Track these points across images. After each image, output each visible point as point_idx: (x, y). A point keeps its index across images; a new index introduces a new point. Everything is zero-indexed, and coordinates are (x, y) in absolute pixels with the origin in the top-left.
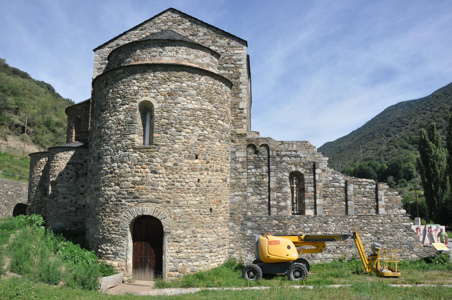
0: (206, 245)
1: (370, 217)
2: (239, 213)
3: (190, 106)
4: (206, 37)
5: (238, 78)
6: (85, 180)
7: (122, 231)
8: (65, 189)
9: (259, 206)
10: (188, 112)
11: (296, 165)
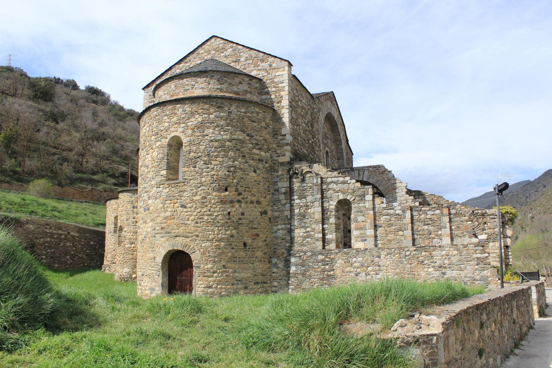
0: (239, 281)
1: (432, 248)
2: (283, 248)
3: (219, 137)
4: (248, 62)
5: (280, 102)
9: (305, 240)
10: (216, 144)
11: (343, 193)
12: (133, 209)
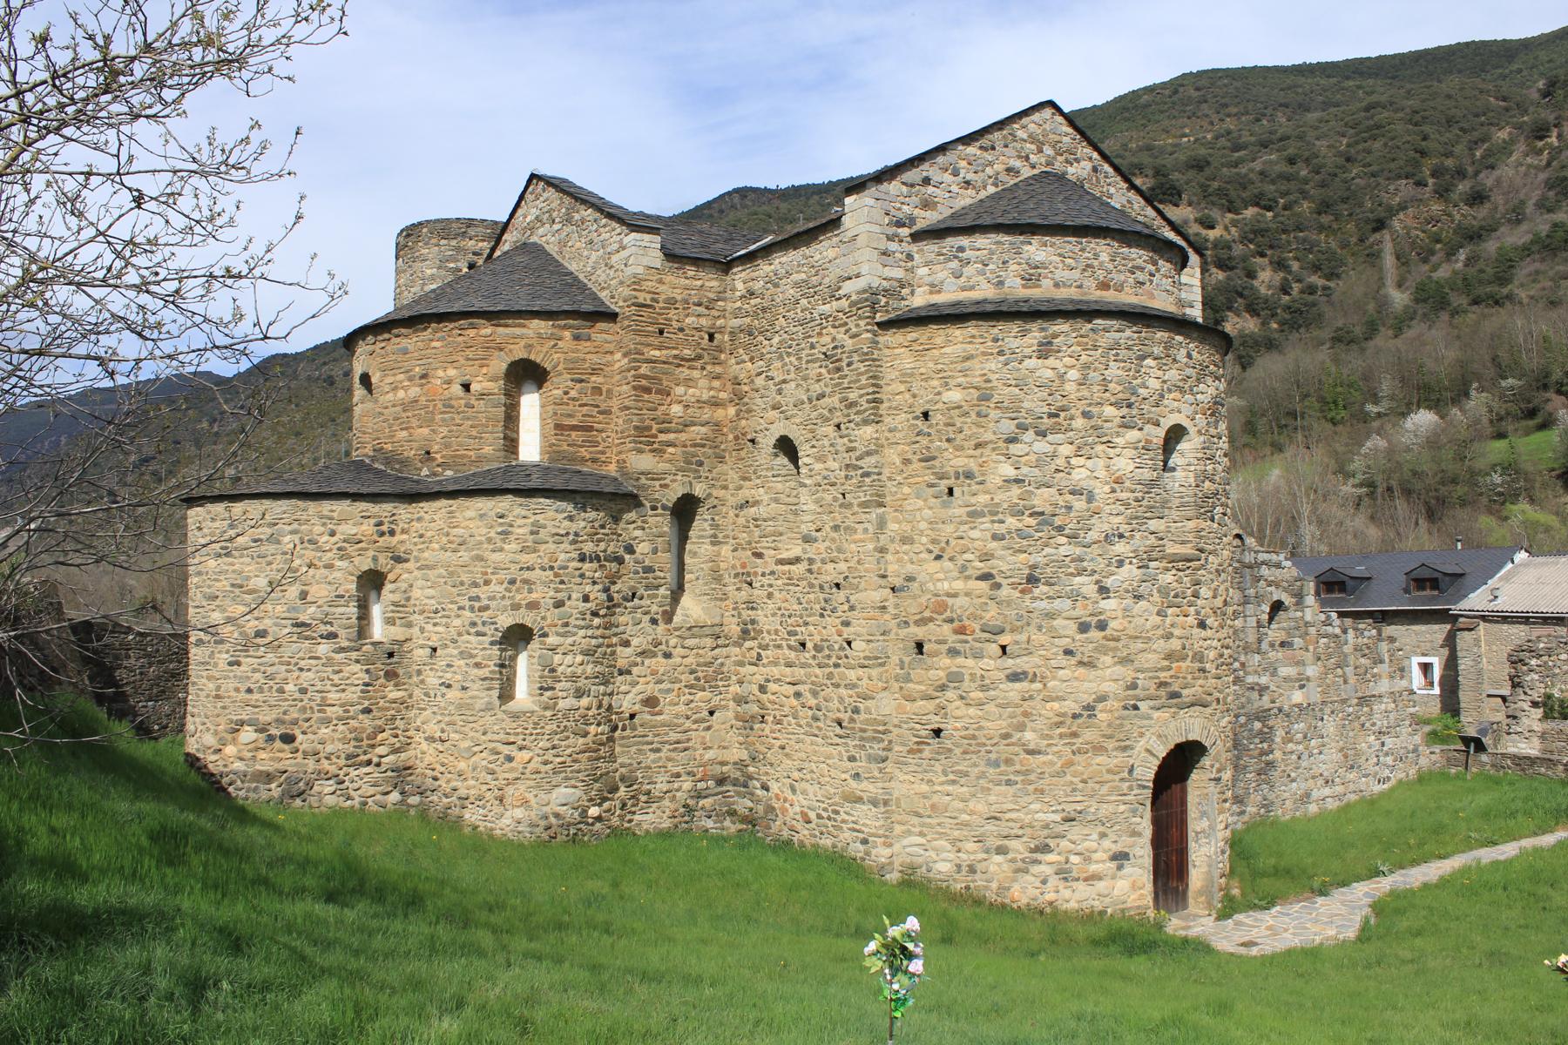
8: (579, 658)
12: (579, 565)
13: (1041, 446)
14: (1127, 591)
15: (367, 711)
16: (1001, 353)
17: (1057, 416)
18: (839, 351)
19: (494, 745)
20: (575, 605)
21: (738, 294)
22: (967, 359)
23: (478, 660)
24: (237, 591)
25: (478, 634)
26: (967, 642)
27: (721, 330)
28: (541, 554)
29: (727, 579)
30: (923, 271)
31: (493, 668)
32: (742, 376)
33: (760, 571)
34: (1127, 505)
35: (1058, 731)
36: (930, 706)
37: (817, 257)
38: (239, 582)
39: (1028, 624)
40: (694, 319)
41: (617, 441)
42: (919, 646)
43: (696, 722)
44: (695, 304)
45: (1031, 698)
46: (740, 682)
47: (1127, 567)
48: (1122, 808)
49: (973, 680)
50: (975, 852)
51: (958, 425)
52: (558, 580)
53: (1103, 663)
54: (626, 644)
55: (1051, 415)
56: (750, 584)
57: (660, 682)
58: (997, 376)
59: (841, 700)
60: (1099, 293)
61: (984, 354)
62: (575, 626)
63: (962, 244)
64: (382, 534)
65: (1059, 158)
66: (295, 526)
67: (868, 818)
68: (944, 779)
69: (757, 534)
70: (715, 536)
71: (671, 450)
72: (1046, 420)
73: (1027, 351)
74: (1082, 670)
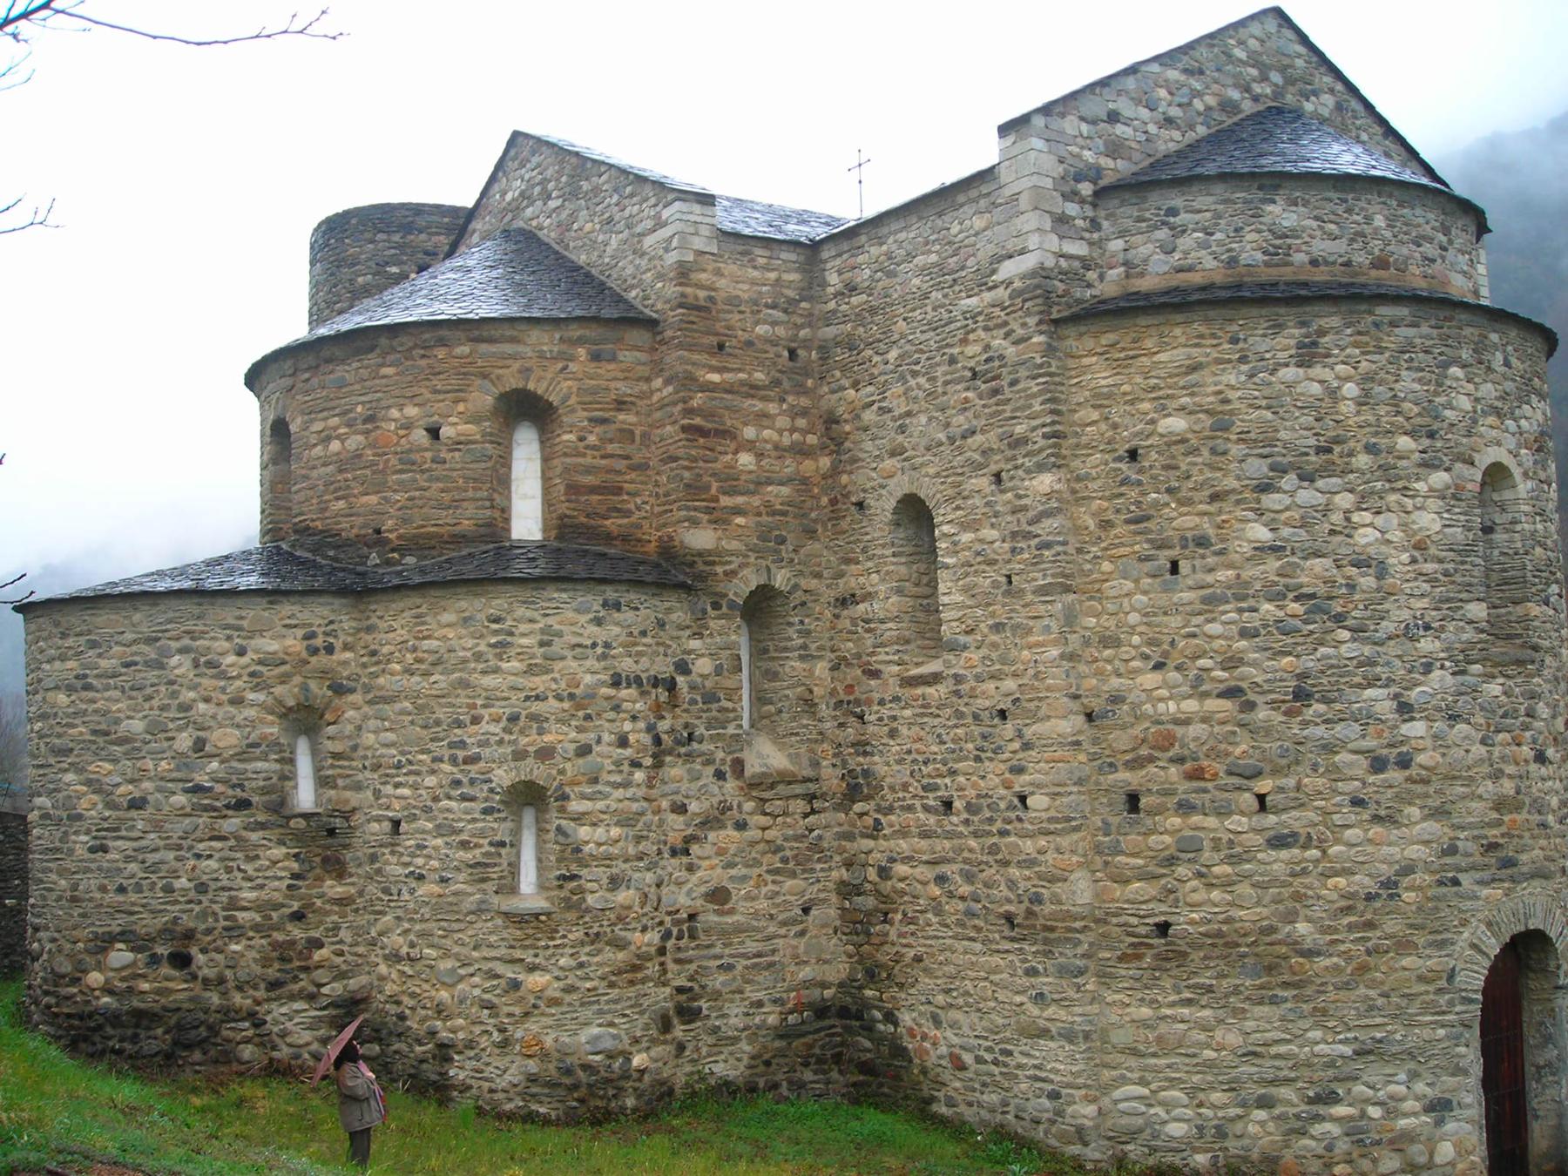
6: (689, 771)
7: (1462, 1008)
8: (615, 832)
12: (611, 692)
13: (1307, 496)
14: (1439, 709)
15: (298, 917)
16: (1243, 359)
17: (1329, 451)
18: (997, 363)
19: (490, 965)
20: (606, 754)
21: (831, 290)
22: (1194, 368)
23: (464, 837)
24: (100, 740)
25: (465, 798)
26: (1205, 791)
27: (807, 344)
28: (557, 676)
29: (824, 710)
30: (1117, 245)
31: (487, 848)
32: (841, 410)
33: (876, 696)
34: (1432, 581)
35: (1346, 921)
36: (1151, 889)
37: (955, 229)
38: (104, 727)
39: (1297, 762)
40: (767, 327)
41: (657, 509)
42: (1133, 801)
43: (784, 924)
44: (767, 306)
45: (1304, 872)
46: (848, 865)
47: (1437, 674)
48: (1441, 1032)
49: (1216, 849)
50: (1225, 1106)
51: (1184, 467)
52: (581, 714)
53: (1409, 816)
54: (680, 809)
55: (1320, 450)
56: (861, 717)
57: (730, 865)
58: (1239, 393)
59: (1012, 885)
60: (1374, 273)
61: (1218, 361)
62: (608, 783)
63: (1172, 203)
64: (314, 651)
65: (1291, 89)
66: (186, 641)
67: (1059, 1060)
68: (1173, 998)
69: (869, 642)
70: (805, 647)
71: (740, 520)
72: (1313, 458)
73: (1282, 356)
74: (1376, 830)
